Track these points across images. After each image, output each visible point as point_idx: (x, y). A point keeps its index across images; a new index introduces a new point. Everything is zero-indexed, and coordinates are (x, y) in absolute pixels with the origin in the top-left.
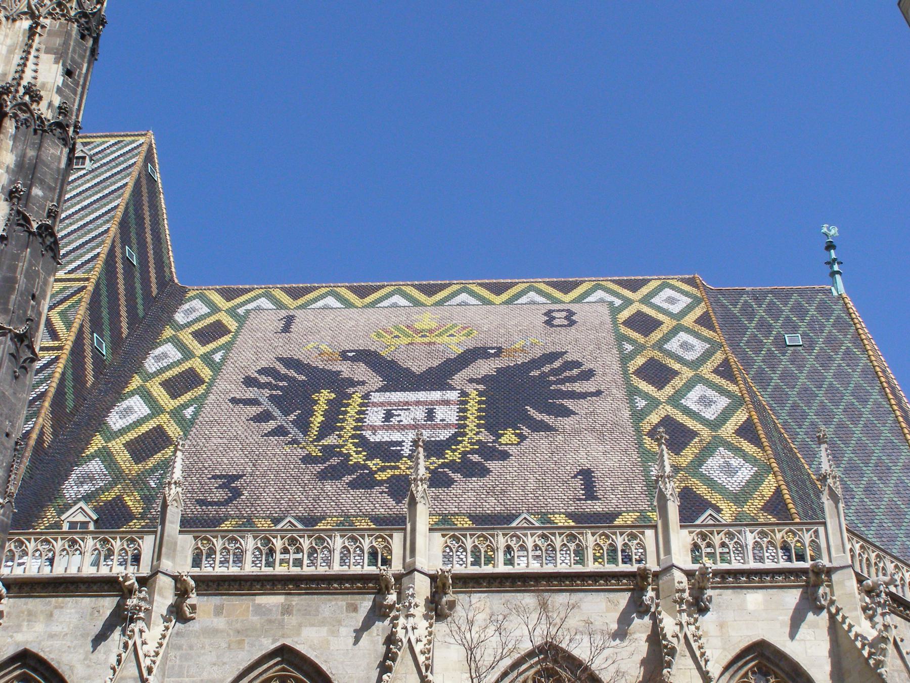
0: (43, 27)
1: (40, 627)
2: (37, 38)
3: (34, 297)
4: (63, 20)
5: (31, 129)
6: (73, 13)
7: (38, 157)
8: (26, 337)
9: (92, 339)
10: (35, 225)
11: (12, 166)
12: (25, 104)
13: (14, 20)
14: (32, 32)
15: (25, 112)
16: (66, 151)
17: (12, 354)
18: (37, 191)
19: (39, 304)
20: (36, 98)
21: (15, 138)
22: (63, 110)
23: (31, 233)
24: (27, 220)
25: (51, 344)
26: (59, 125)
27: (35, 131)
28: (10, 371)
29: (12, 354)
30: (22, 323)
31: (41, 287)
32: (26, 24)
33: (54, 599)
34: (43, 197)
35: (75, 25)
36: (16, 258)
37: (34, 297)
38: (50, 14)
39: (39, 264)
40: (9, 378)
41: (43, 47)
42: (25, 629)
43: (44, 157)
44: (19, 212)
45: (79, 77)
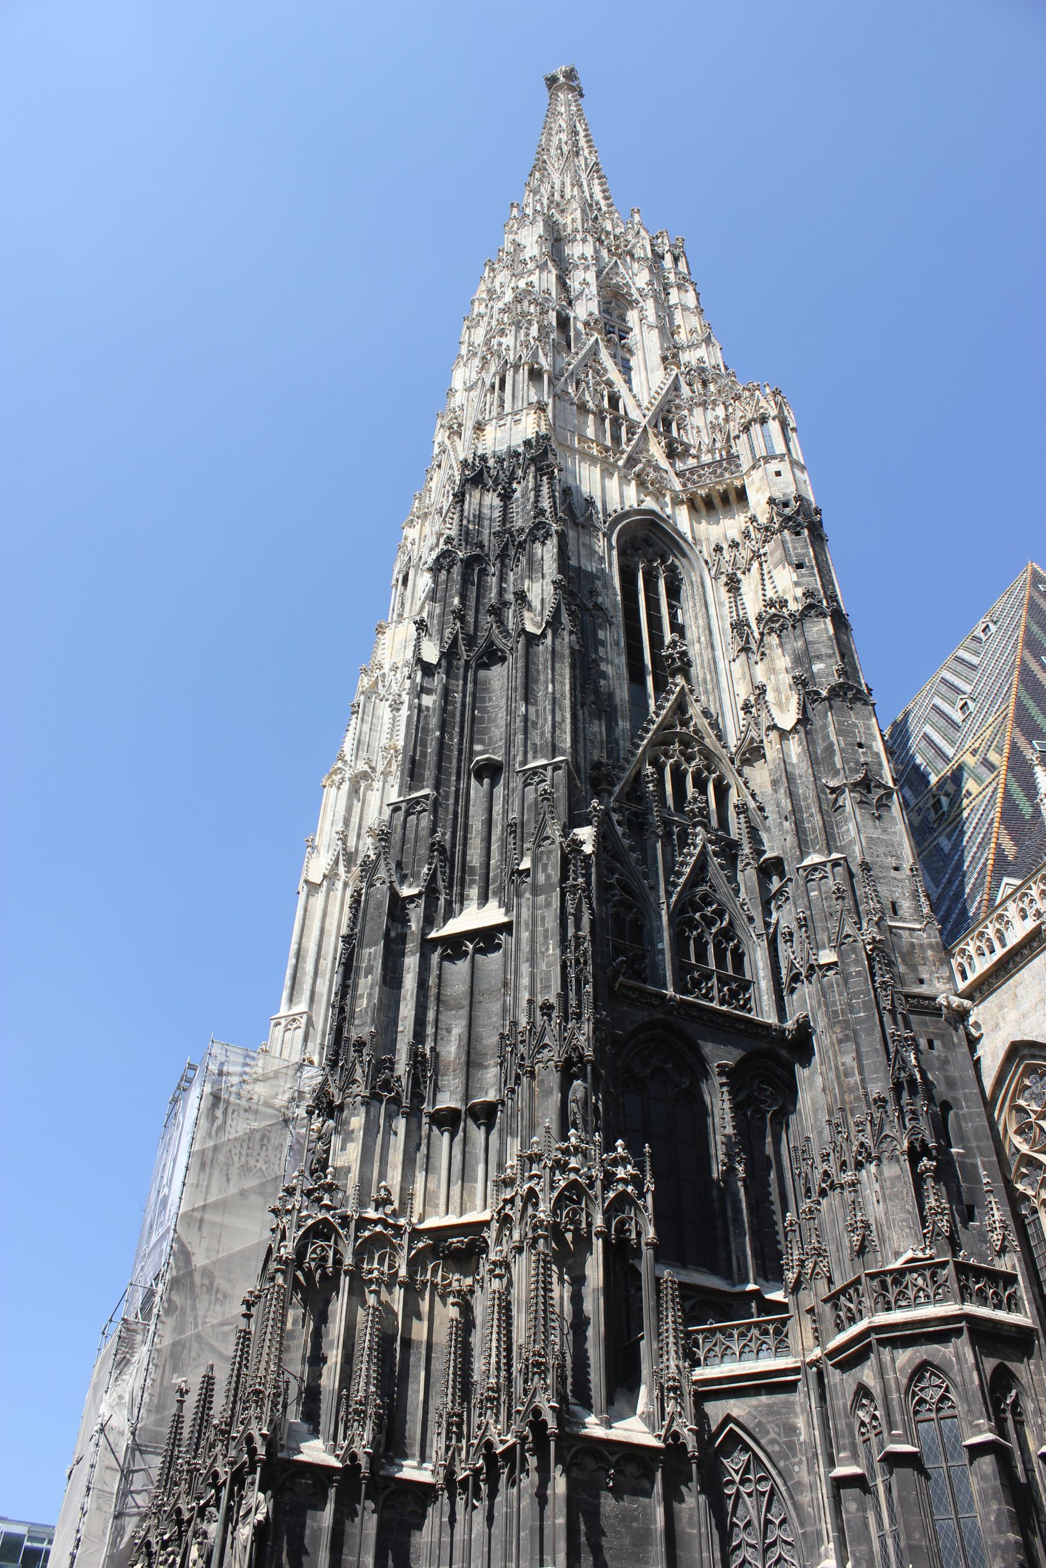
0: (765, 554)
1: (1012, 1015)
2: (765, 565)
3: (860, 746)
4: (775, 537)
5: (790, 628)
6: (776, 526)
7: (805, 641)
8: (871, 780)
9: (1033, 748)
10: (824, 693)
11: (789, 665)
12: (775, 615)
13: (749, 570)
14: (761, 564)
15: (778, 621)
16: (828, 620)
17: (861, 802)
18: (817, 667)
19: (870, 747)
20: (784, 603)
21: (781, 645)
22: (808, 594)
23: (824, 700)
24: (817, 693)
25: (993, 776)
26: (810, 607)
27: (793, 626)
28: (867, 816)
29: (861, 802)
30: (858, 772)
31: (865, 733)
32: (756, 565)
33: (1011, 981)
34: (826, 667)
35: (786, 531)
36: (825, 727)
37: (860, 746)
38: (765, 541)
39: (850, 717)
40: (870, 822)
41: (771, 567)
42: (1002, 1024)
43: (809, 638)
44: (808, 693)
45: (810, 562)
